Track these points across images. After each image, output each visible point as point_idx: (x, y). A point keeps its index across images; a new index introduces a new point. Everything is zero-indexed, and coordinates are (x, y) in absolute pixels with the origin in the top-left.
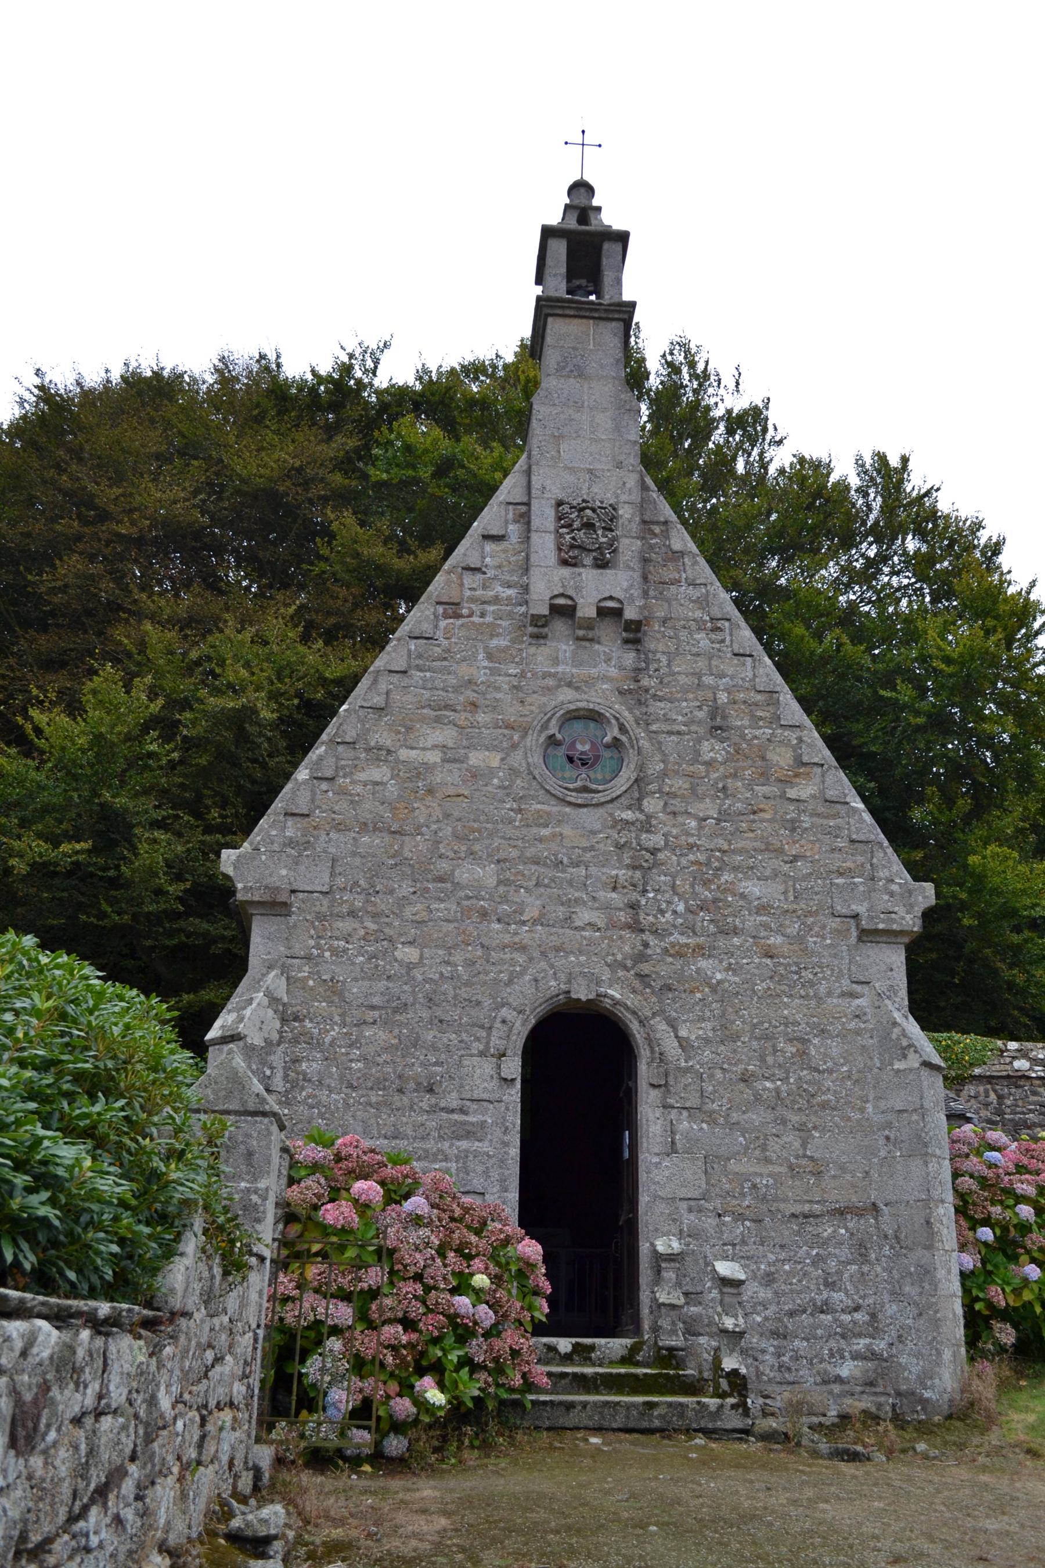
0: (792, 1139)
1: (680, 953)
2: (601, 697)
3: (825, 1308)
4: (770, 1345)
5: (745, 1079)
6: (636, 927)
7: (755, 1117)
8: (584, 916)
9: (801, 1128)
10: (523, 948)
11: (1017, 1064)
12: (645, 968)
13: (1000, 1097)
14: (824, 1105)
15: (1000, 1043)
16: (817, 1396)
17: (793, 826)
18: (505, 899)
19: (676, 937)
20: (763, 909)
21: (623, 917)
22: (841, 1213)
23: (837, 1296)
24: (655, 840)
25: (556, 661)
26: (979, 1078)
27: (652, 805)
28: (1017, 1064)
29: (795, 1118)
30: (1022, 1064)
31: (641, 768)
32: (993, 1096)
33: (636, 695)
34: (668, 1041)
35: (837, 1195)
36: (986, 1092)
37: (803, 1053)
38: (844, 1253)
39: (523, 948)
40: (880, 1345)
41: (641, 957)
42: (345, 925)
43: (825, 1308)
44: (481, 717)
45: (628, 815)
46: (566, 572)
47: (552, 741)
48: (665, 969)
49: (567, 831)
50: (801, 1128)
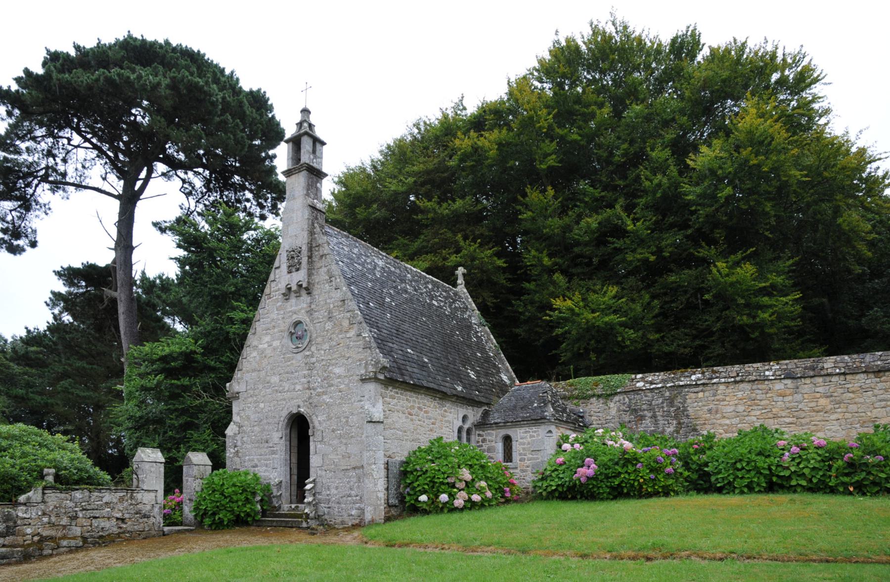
0: (343, 447)
1: (319, 395)
2: (303, 317)
3: (349, 496)
4: (336, 506)
5: (333, 431)
6: (309, 389)
7: (336, 442)
8: (298, 387)
9: (346, 444)
10: (285, 400)
11: (638, 385)
12: (311, 401)
13: (630, 400)
14: (352, 437)
15: (633, 376)
16: (346, 519)
17: (348, 347)
18: (281, 386)
19: (319, 390)
20: (339, 377)
21: (306, 386)
22: (354, 468)
23: (353, 492)
24: (314, 360)
25: (291, 306)
26: (620, 393)
27: (313, 348)
28: (638, 385)
29: (344, 441)
30: (640, 384)
31: (311, 337)
32: (627, 400)
33: (310, 312)
34: (318, 422)
35: (354, 464)
36: (624, 399)
37: (347, 421)
38: (355, 480)
39: (285, 400)
40: (362, 506)
41: (310, 398)
42: (250, 400)
43: (349, 496)
44: (276, 330)
45: (308, 353)
46: (289, 275)
47: (292, 334)
48: (315, 400)
49: (294, 362)
50: (346, 444)
